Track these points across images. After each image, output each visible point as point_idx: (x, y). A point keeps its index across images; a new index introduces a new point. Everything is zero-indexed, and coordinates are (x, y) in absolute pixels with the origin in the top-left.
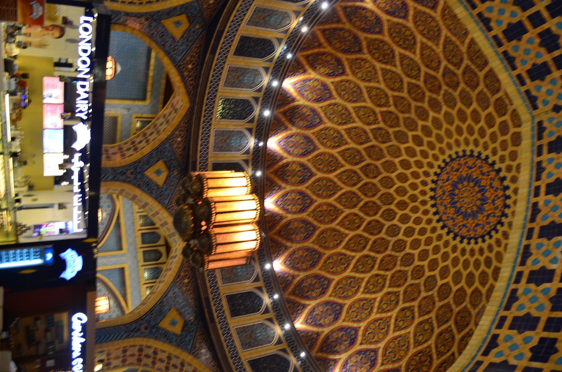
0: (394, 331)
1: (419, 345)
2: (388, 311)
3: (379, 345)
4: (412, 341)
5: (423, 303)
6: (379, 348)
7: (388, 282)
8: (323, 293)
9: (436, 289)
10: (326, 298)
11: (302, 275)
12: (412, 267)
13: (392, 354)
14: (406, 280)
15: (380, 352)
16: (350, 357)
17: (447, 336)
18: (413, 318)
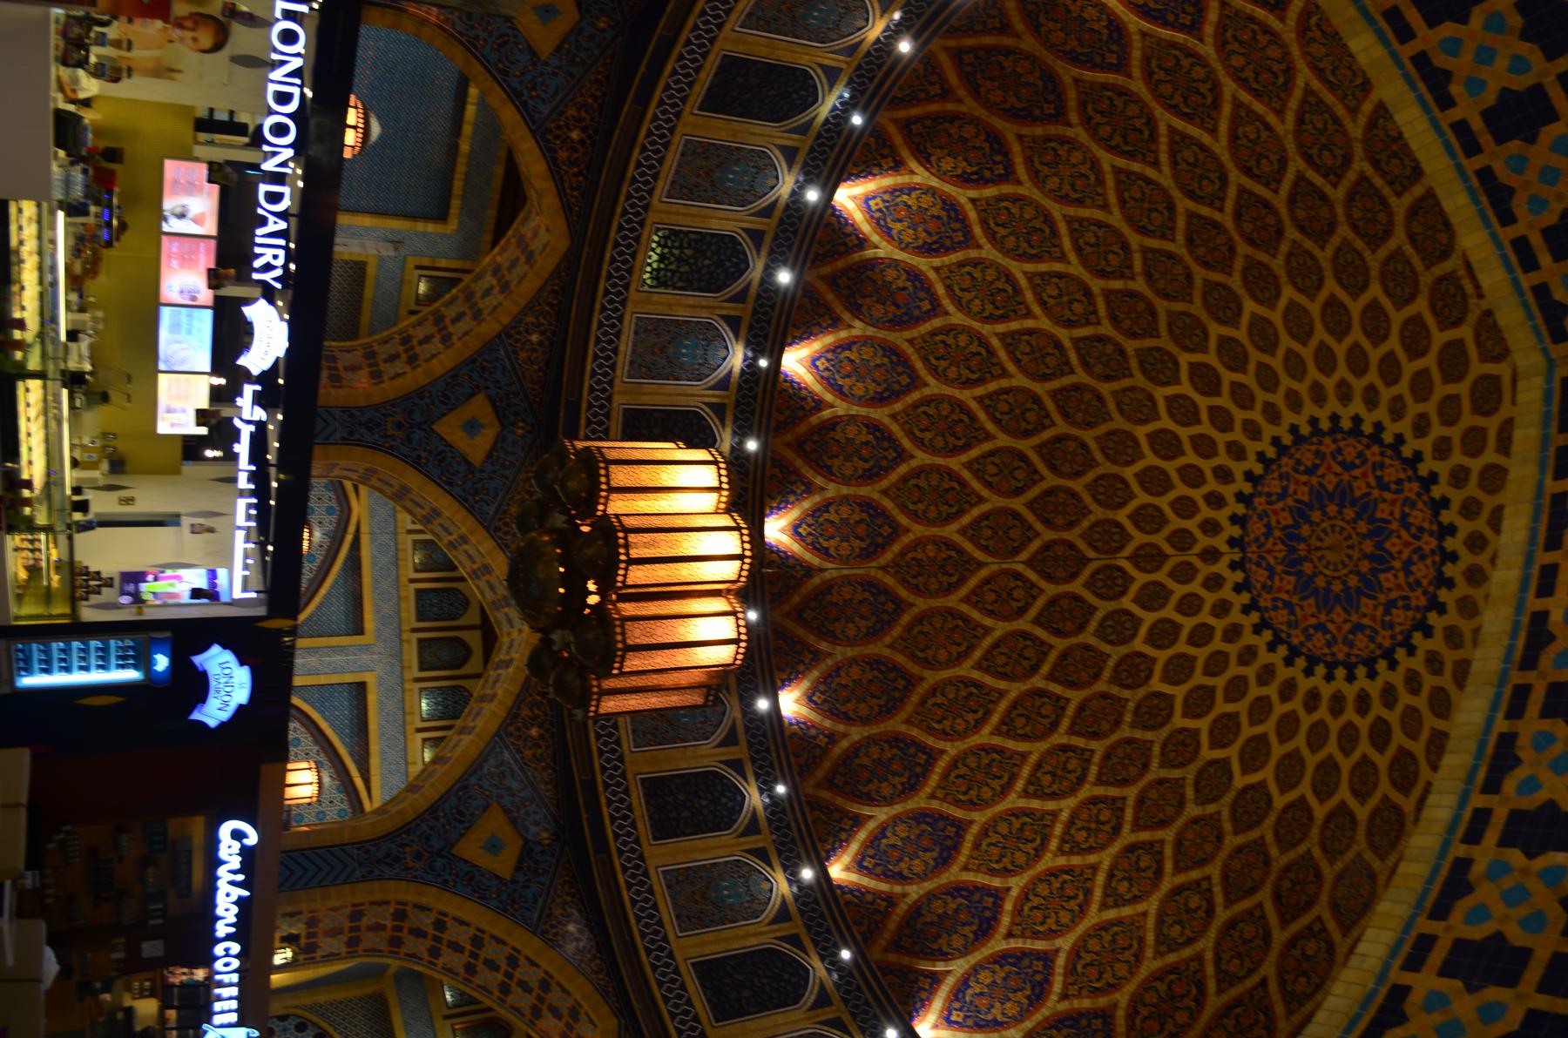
0: (1104, 906)
3: (1058, 942)
4: (1150, 938)
6: (1057, 951)
8: (911, 788)
9: (1228, 798)
10: (918, 802)
11: (857, 733)
12: (1165, 732)
13: (1093, 970)
14: (1146, 766)
15: (1061, 961)
16: (976, 969)
17: (1249, 930)
18: (1159, 873)
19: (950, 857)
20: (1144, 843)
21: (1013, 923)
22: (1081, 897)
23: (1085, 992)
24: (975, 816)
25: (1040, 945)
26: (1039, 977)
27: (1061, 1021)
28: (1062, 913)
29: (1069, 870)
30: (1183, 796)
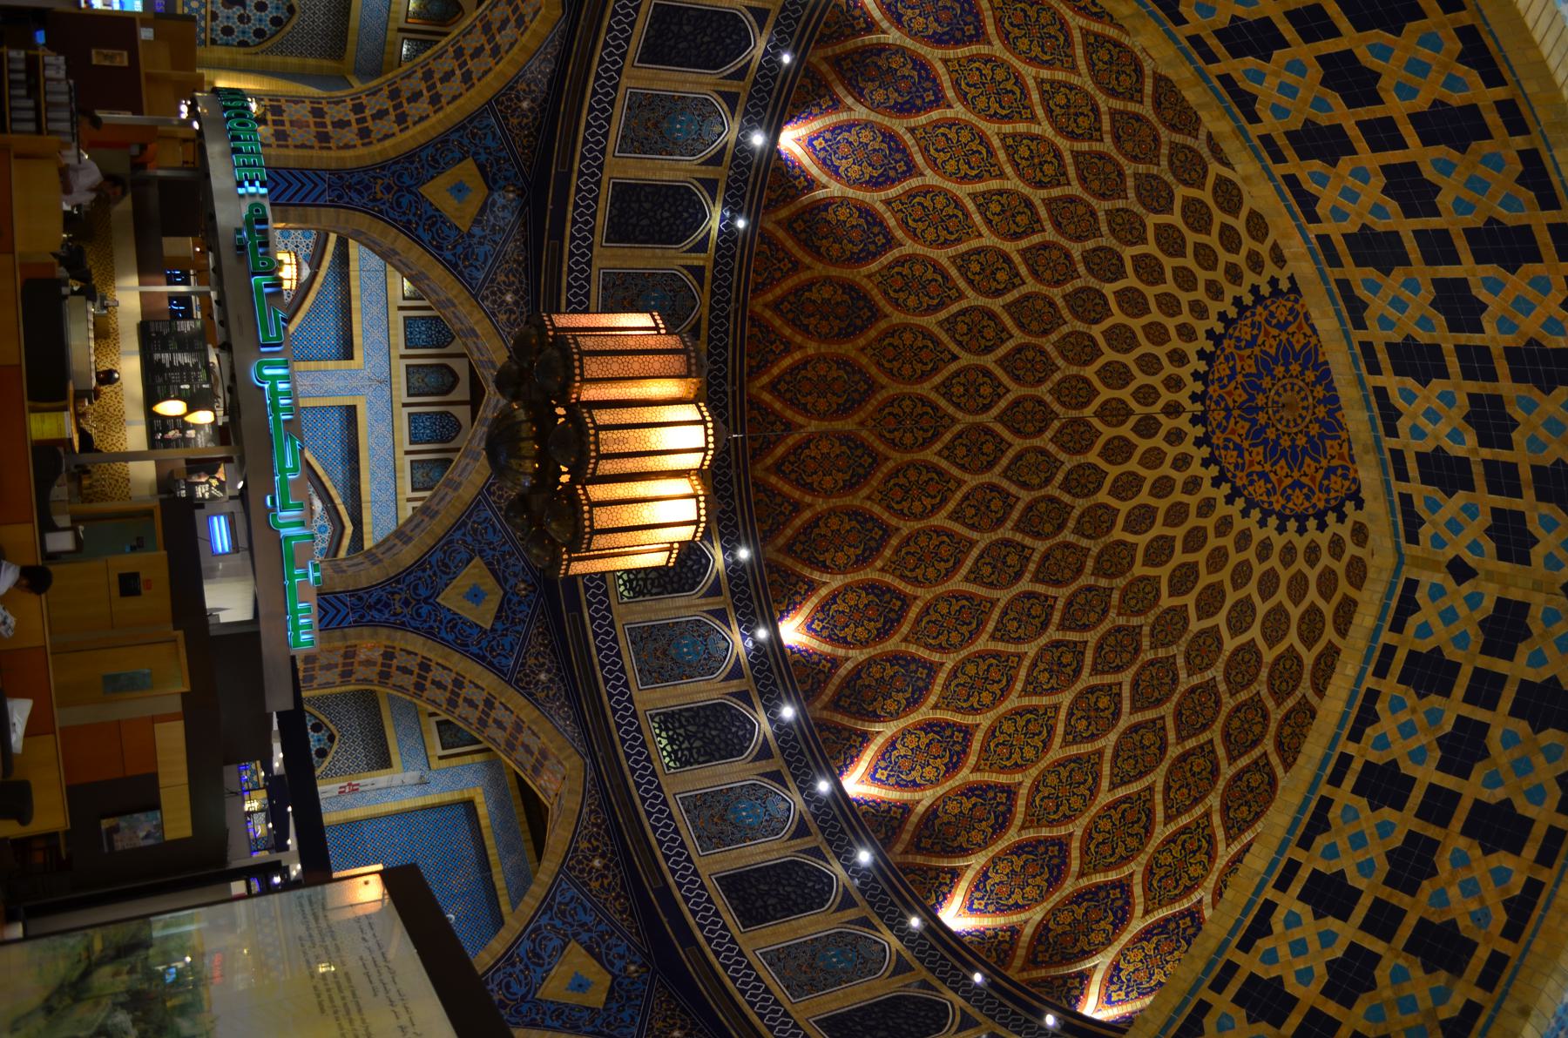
1: (959, 269)
2: (1016, 165)
3: (928, 172)
4: (963, 248)
5: (1055, 254)
6: (922, 174)
7: (1084, 146)
12: (1138, 209)
13: (919, 212)
14: (1103, 196)
15: (914, 182)
16: (867, 125)
19: (947, 42)
20: (1037, 213)
21: (924, 127)
22: (974, 173)
24: (997, 43)
25: (919, 159)
26: (892, 173)
27: (867, 212)
28: (953, 162)
29: (991, 152)
30: (1087, 238)
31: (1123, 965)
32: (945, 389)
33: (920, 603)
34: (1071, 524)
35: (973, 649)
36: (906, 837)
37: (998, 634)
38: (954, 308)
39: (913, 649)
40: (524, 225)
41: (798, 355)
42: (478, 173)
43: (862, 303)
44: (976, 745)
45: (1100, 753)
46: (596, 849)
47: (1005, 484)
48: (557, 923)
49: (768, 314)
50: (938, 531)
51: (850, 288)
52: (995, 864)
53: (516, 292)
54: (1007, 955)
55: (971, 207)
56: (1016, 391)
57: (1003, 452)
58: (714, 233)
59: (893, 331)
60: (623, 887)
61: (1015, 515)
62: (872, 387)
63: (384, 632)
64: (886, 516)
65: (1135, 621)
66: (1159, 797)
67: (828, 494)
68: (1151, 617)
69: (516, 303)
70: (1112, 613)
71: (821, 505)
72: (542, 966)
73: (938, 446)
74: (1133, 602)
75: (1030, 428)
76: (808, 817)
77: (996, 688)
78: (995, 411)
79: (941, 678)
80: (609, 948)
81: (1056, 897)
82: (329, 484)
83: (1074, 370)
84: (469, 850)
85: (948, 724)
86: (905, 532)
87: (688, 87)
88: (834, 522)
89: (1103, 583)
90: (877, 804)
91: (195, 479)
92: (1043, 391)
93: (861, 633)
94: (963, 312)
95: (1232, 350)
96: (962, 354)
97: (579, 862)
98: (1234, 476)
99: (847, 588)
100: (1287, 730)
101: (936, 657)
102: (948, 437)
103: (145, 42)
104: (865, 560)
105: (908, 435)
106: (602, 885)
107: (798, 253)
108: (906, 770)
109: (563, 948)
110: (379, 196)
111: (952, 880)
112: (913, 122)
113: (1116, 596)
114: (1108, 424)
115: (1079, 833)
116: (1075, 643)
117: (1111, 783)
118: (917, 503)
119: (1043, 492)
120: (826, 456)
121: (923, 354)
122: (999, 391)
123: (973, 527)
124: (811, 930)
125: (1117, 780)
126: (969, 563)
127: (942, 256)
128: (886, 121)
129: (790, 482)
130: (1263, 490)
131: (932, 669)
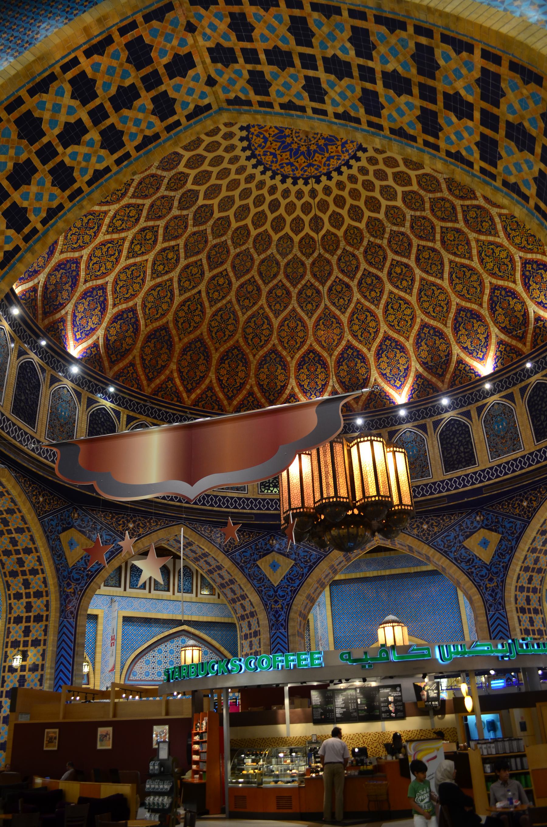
1: (158, 277)
3: (107, 279)
4: (149, 272)
5: (172, 224)
6: (107, 283)
9: (194, 209)
15: (109, 288)
17: (195, 270)
18: (155, 242)
21: (86, 274)
23: (122, 301)
30: (172, 205)
31: (539, 300)
32: (213, 301)
33: (314, 344)
34: (304, 258)
35: (346, 324)
36: (434, 380)
37: (343, 310)
38: (176, 285)
39: (336, 353)
40: (93, 510)
41: (175, 375)
42: (66, 532)
43: (158, 334)
44: (395, 336)
45: (422, 279)
46: (418, 526)
47: (271, 285)
48: (453, 549)
49: (153, 386)
50: (281, 325)
51: (149, 338)
52: (460, 342)
53: (128, 521)
54: (514, 349)
55: (132, 261)
56: (227, 266)
57: (255, 281)
58: (112, 405)
59: (176, 320)
60: (439, 516)
61: (288, 284)
62: (200, 339)
63: (292, 615)
64: (265, 349)
65: (365, 243)
66: (457, 259)
67: (247, 376)
68: (366, 234)
69: (134, 522)
70: (356, 252)
71: (252, 381)
72: (473, 560)
73: (240, 314)
74: (355, 241)
75: (249, 264)
76: (416, 423)
77: (369, 318)
78: (233, 280)
79: (355, 343)
80: (467, 528)
81: (488, 320)
82: (162, 636)
83: (230, 233)
84: (354, 587)
85: (380, 346)
86: (276, 342)
87: (47, 403)
88: (262, 376)
89: (339, 252)
90: (413, 390)
91: (425, 697)
92: (233, 252)
93: (322, 376)
94: (179, 281)
95: (262, 151)
96: (199, 288)
97: (424, 535)
98: (320, 172)
99: (297, 378)
100: (457, 192)
101: (344, 343)
102: (237, 307)
103: (31, 719)
104: (285, 366)
105: (229, 327)
106: (437, 526)
107: (126, 361)
108: (398, 372)
109: (466, 549)
110: (72, 590)
111: (463, 364)
112: (82, 280)
113: (348, 248)
114: (263, 224)
115: (458, 300)
116: (363, 274)
117: (439, 278)
118: (264, 332)
119: (282, 268)
120: (228, 372)
121: (192, 308)
122: (224, 275)
123: (286, 307)
124: (481, 434)
125: (439, 275)
126: (302, 314)
127: (149, 283)
128: (77, 294)
129: (238, 394)
130: (335, 161)
131: (349, 346)
